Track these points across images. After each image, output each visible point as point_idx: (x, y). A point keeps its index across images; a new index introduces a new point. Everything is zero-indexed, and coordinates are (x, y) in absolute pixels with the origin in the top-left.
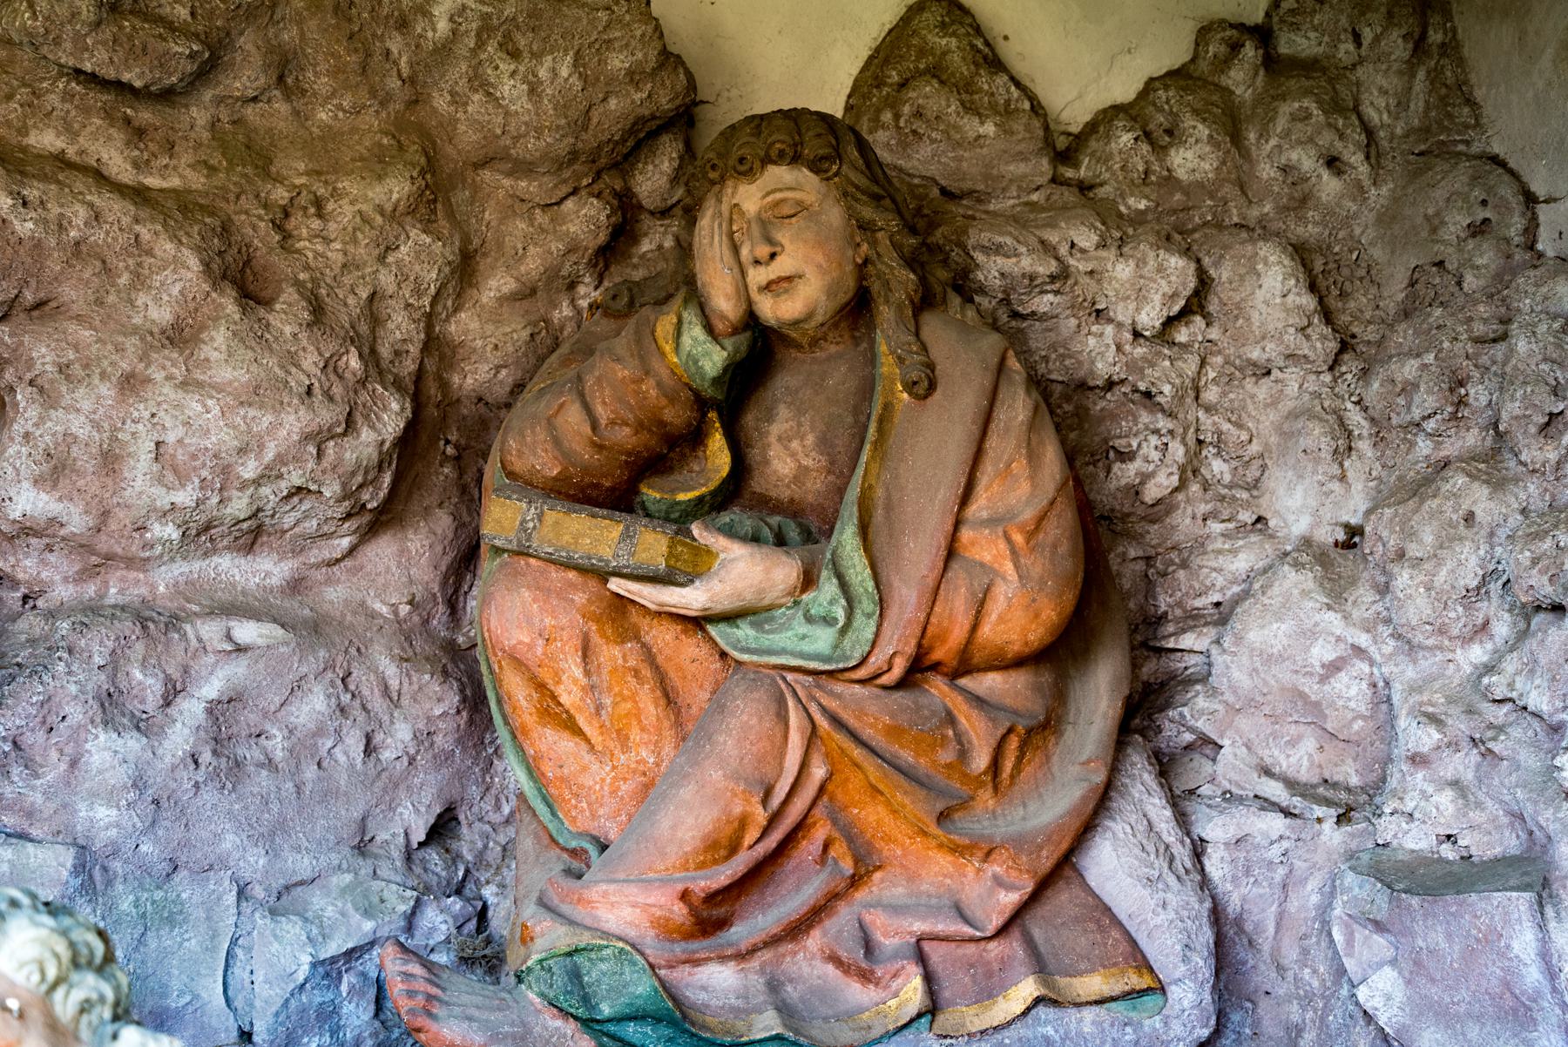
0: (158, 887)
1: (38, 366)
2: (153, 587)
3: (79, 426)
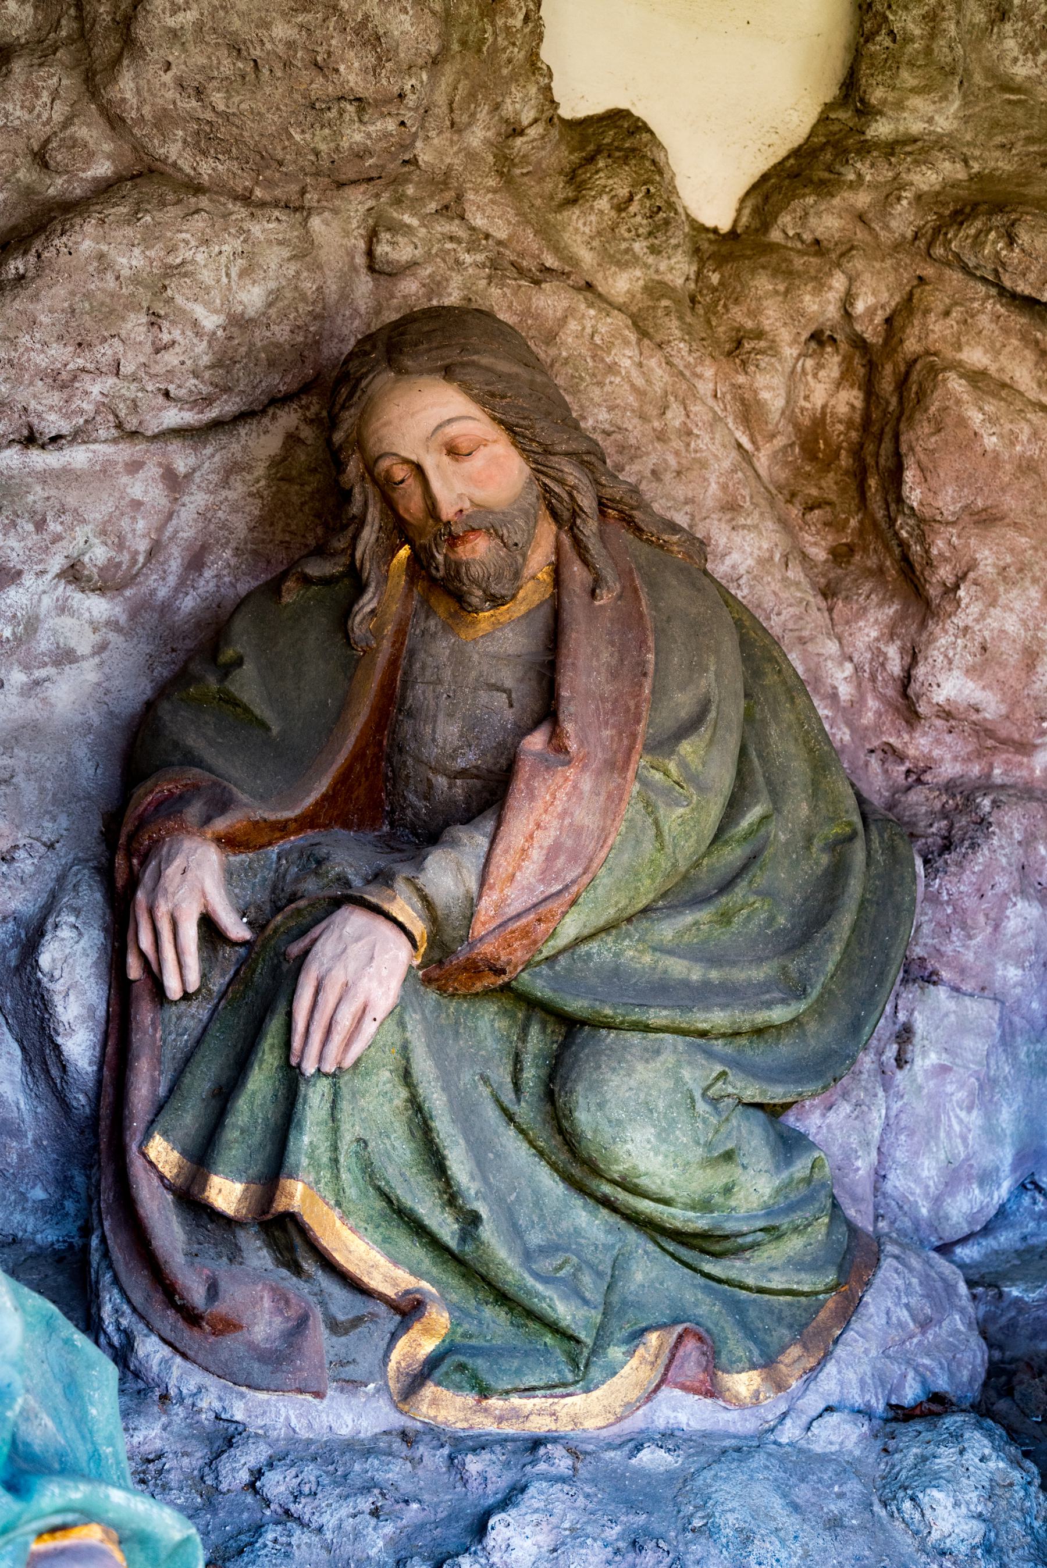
0: (1038, 1041)
1: (981, 567)
2: (1032, 770)
3: (1012, 625)
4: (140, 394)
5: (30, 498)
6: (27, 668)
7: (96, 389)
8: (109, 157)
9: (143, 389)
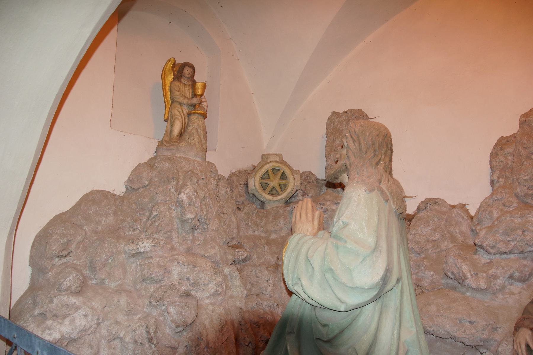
4: (522, 245)
5: (502, 263)
6: (503, 295)
7: (513, 244)
8: (517, 203)
9: (522, 244)
